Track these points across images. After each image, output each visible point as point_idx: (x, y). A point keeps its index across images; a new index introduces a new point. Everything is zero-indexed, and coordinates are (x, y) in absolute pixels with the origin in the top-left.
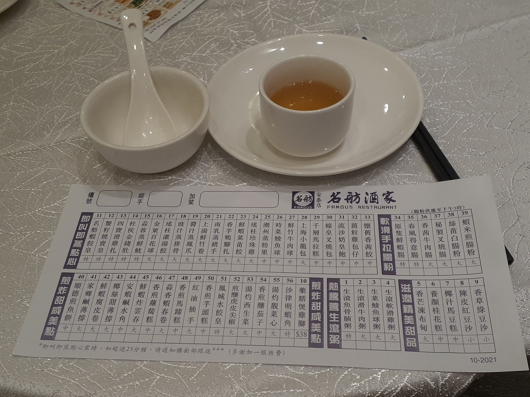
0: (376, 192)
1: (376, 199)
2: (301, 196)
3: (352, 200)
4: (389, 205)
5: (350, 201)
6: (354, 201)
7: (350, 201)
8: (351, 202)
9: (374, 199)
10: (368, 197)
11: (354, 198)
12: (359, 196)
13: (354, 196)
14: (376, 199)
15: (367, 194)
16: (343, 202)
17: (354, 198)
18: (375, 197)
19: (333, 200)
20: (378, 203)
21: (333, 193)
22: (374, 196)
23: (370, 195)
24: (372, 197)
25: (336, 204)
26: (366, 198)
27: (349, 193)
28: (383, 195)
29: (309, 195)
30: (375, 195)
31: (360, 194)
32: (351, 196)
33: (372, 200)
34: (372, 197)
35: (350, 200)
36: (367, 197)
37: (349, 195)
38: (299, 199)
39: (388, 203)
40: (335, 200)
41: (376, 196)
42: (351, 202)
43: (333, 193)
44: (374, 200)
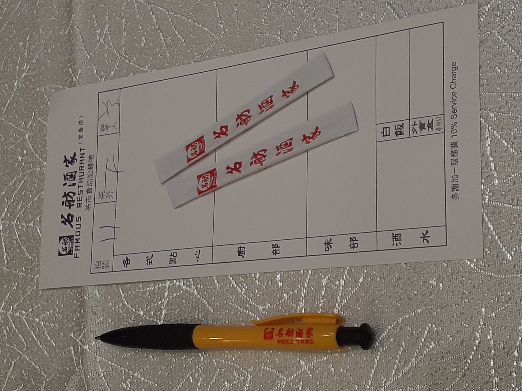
0: (64, 175)
1: (72, 174)
2: (63, 248)
4: (79, 159)
5: (72, 202)
6: (72, 198)
7: (72, 202)
8: (74, 201)
9: (71, 176)
10: (69, 183)
11: (69, 198)
12: (67, 193)
14: (72, 174)
17: (69, 198)
18: (69, 176)
19: (70, 222)
20: (76, 172)
21: (62, 222)
22: (68, 177)
24: (69, 179)
26: (69, 186)
27: (63, 204)
28: (67, 166)
29: (62, 241)
30: (67, 175)
31: (65, 193)
33: (73, 179)
34: (69, 179)
35: (71, 203)
36: (68, 184)
37: (66, 204)
38: (65, 250)
39: (77, 160)
40: (70, 219)
41: (68, 174)
42: (74, 201)
43: (62, 222)
44: (72, 176)
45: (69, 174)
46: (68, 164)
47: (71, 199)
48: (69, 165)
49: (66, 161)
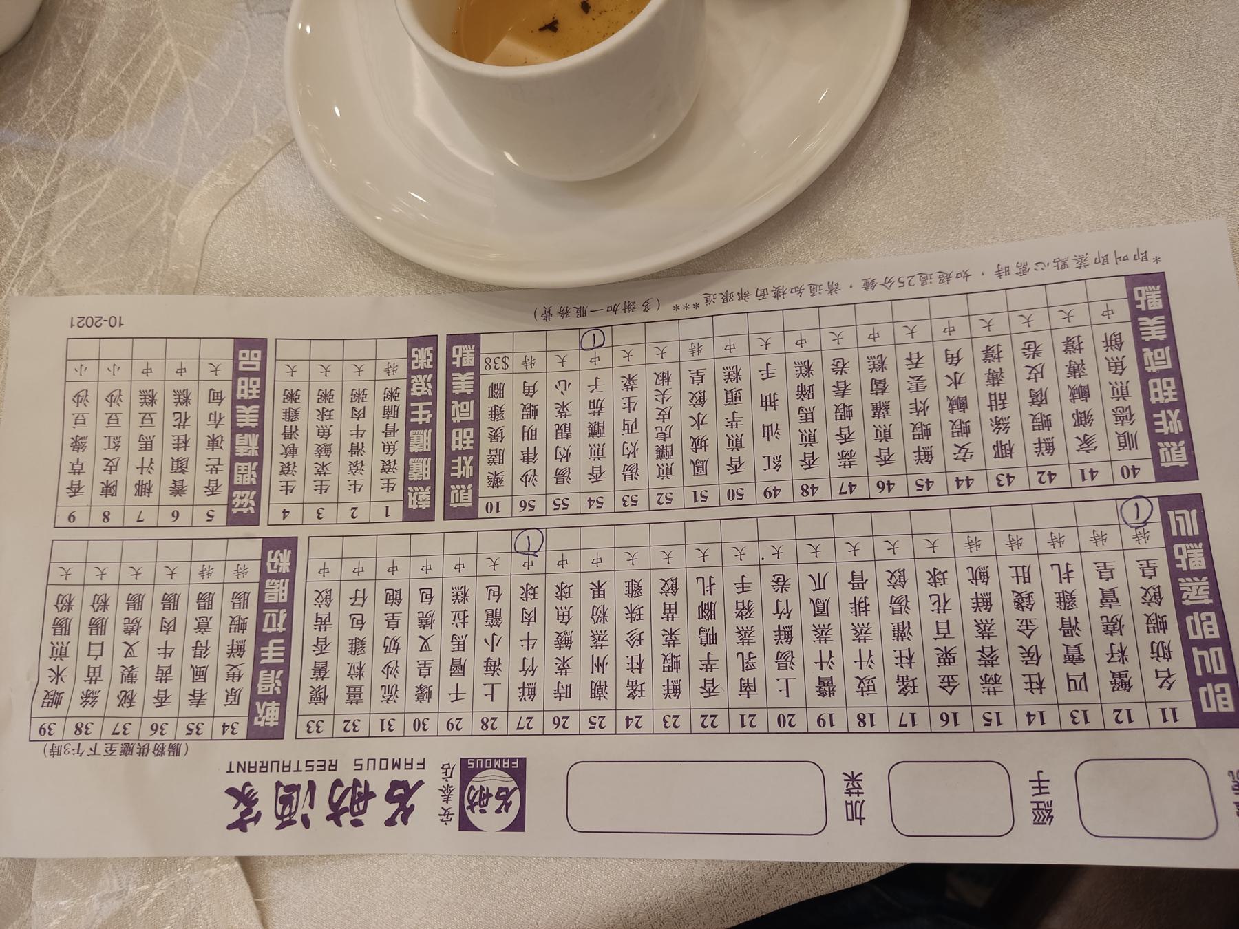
3: (354, 792)
7: (359, 790)
8: (356, 783)
13: (345, 810)
15: (306, 822)
16: (380, 783)
22: (287, 812)
23: (297, 818)
24: (293, 810)
25: (400, 775)
26: (311, 805)
28: (256, 819)
32: (356, 810)
33: (295, 795)
34: (293, 810)
42: (356, 783)
45: (280, 806)
46: (253, 815)
47: (350, 793)
48: (256, 809)
49: (241, 825)
